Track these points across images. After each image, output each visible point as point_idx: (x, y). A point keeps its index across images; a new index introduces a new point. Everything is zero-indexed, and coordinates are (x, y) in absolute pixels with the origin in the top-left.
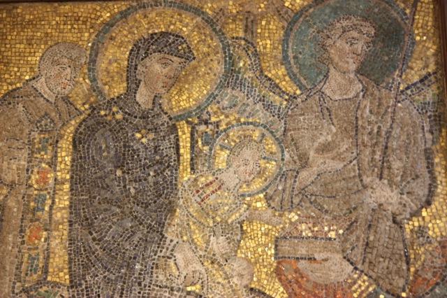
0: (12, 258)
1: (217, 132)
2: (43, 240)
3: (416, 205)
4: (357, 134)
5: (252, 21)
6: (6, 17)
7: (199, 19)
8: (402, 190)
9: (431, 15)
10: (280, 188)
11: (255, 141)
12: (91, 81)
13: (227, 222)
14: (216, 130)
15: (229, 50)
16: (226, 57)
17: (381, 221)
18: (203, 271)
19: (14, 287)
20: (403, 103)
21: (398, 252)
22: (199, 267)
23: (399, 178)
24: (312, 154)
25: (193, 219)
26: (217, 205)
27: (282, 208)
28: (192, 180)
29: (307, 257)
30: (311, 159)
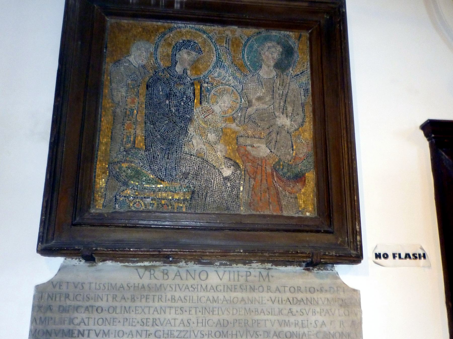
8: (292, 120)
15: (218, 51)
23: (290, 114)
24: (254, 101)
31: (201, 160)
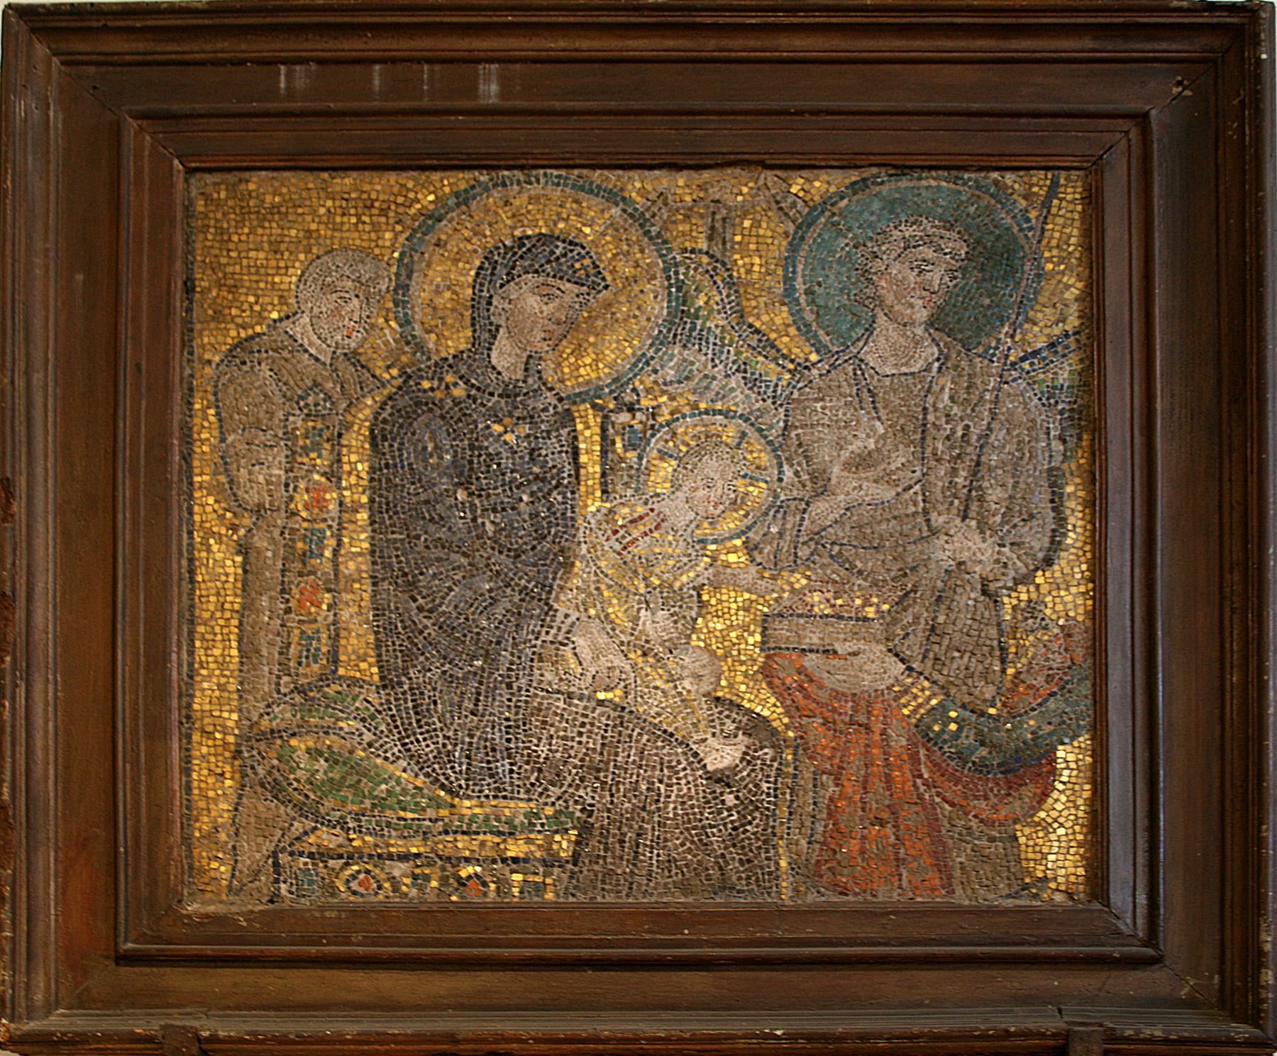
0: (270, 636)
1: (652, 427)
3: (1026, 565)
4: (923, 439)
5: (724, 220)
6: (228, 198)
7: (616, 211)
8: (1002, 538)
9: (1077, 224)
10: (774, 530)
11: (727, 445)
12: (401, 326)
13: (671, 586)
14: (651, 422)
15: (677, 273)
16: (671, 286)
17: (959, 590)
18: (628, 668)
19: (278, 684)
20: (1014, 384)
21: (988, 642)
22: (618, 661)
23: (998, 519)
24: (836, 470)
25: (606, 580)
26: (652, 558)
27: (776, 564)
28: (604, 511)
29: (821, 649)
30: (834, 481)
31: (613, 714)
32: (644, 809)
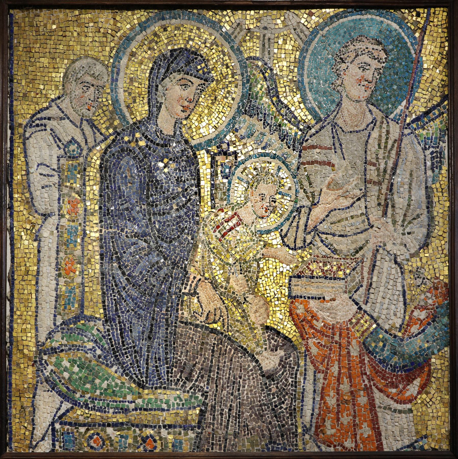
2: (77, 273)
32: (232, 394)
